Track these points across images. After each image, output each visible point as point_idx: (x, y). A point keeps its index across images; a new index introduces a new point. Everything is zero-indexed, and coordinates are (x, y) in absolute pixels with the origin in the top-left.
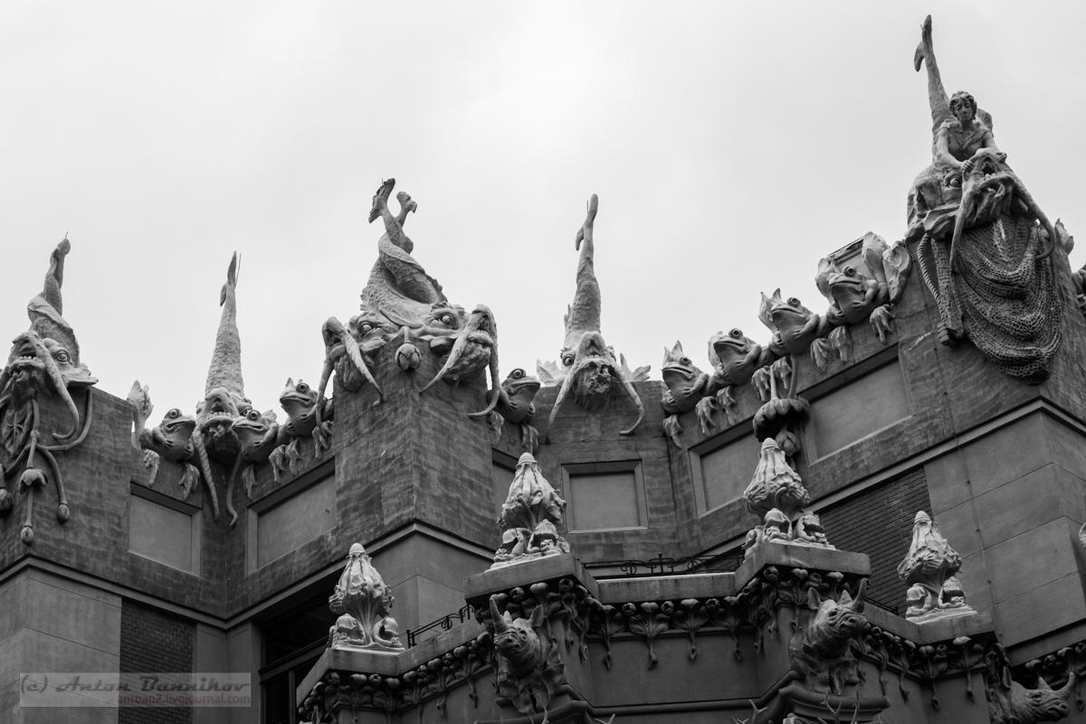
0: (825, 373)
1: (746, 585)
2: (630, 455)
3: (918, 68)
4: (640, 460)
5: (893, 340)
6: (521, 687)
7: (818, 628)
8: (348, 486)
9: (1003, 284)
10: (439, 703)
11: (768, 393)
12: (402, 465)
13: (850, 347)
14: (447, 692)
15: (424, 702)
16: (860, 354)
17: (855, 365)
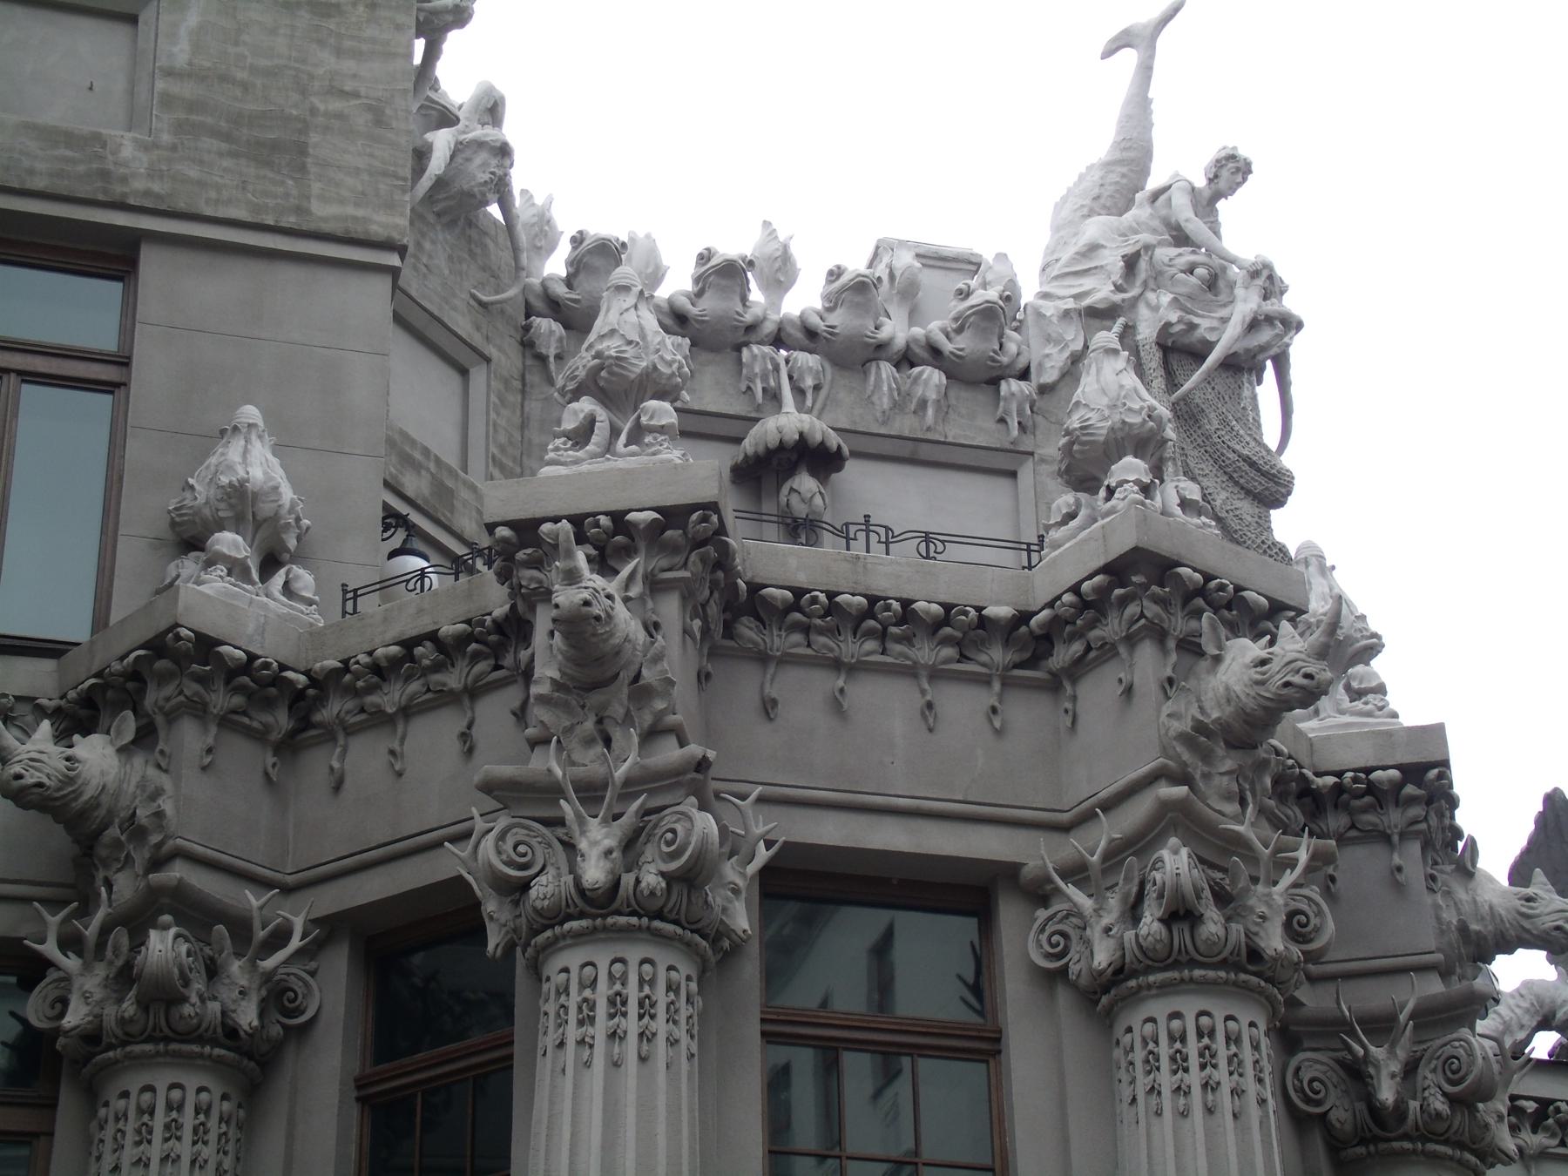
0: (884, 423)
1: (1368, 771)
2: (477, 340)
3: (1108, 53)
4: (488, 360)
5: (1027, 444)
6: (1228, 765)
7: (1491, 908)
8: (190, 74)
9: (1264, 474)
10: (824, 682)
11: (774, 396)
12: (379, 122)
13: (944, 407)
14: (854, 669)
15: (787, 660)
16: (954, 432)
17: (944, 443)
